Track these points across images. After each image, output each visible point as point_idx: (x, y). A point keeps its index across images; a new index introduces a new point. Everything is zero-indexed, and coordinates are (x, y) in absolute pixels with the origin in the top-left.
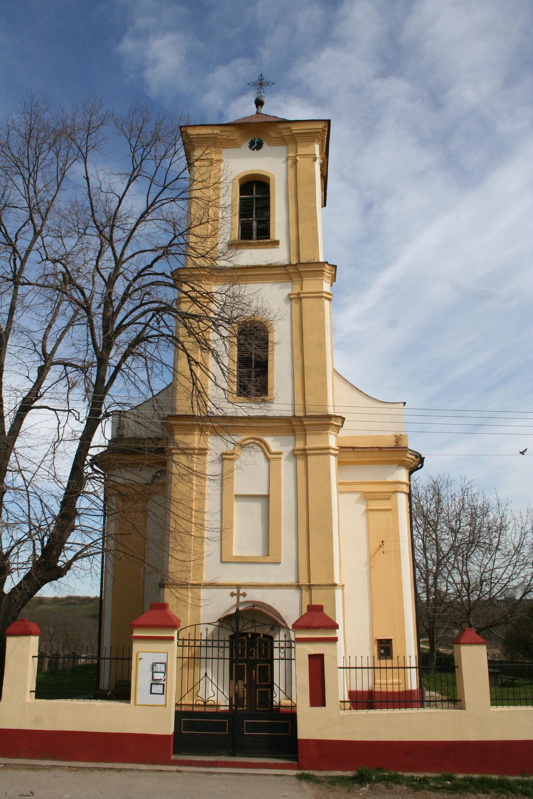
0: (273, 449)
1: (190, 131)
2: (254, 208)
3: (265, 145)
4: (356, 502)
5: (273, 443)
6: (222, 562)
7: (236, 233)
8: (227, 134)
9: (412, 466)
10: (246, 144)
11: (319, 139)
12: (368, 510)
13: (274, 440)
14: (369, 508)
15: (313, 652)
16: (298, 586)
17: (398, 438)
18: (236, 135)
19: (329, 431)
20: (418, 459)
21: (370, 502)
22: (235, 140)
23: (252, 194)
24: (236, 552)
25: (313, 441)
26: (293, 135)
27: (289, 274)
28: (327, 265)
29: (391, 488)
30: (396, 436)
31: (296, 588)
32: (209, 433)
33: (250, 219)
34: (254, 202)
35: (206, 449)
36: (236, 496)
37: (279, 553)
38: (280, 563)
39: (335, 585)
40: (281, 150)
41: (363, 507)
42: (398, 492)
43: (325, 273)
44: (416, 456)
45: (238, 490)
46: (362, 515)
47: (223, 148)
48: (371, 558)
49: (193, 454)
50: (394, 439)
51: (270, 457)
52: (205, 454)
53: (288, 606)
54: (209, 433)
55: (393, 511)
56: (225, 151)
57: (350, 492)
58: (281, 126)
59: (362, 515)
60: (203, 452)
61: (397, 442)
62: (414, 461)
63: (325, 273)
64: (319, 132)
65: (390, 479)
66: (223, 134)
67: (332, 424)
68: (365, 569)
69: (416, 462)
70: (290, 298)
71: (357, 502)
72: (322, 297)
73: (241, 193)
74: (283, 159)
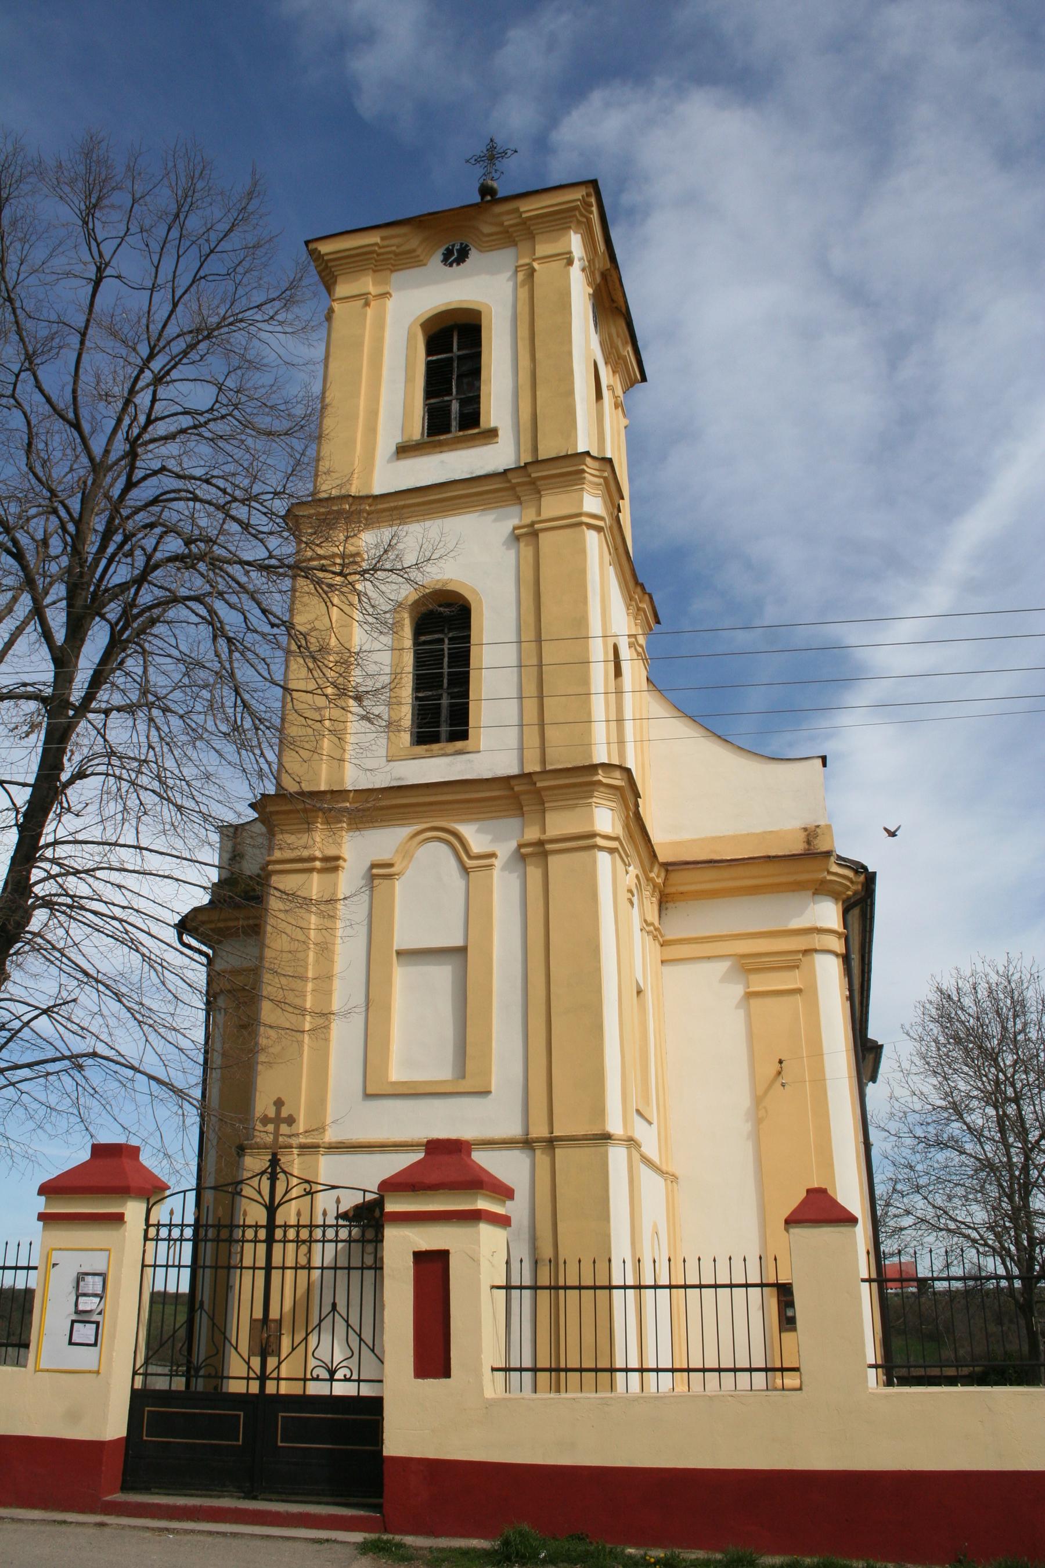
0: (476, 848)
2: (455, 377)
3: (474, 254)
4: (724, 979)
5: (476, 836)
6: (368, 1096)
7: (417, 429)
9: (850, 893)
10: (438, 256)
11: (579, 222)
12: (750, 995)
13: (478, 831)
14: (751, 989)
15: (424, 1246)
16: (527, 1143)
17: (811, 834)
18: (413, 241)
19: (594, 800)
20: (862, 878)
21: (753, 977)
22: (414, 251)
23: (451, 351)
24: (396, 1074)
25: (560, 823)
26: (524, 222)
27: (513, 488)
28: (588, 460)
30: (805, 829)
31: (522, 1148)
32: (345, 825)
33: (446, 398)
34: (455, 365)
35: (337, 858)
36: (399, 953)
37: (486, 1073)
38: (489, 1092)
39: (607, 1137)
40: (506, 258)
41: (738, 990)
42: (816, 951)
43: (586, 475)
44: (856, 872)
45: (402, 940)
46: (738, 1007)
47: (392, 271)
48: (758, 1101)
49: (311, 870)
50: (802, 836)
51: (470, 865)
52: (336, 869)
54: (345, 825)
55: (806, 993)
56: (395, 277)
57: (709, 958)
59: (738, 1007)
60: (332, 864)
61: (809, 842)
63: (586, 475)
64: (576, 208)
65: (795, 924)
66: (386, 243)
67: (600, 783)
68: (747, 1127)
69: (858, 883)
70: (516, 537)
71: (724, 979)
72: (581, 524)
73: (429, 352)
74: (509, 274)
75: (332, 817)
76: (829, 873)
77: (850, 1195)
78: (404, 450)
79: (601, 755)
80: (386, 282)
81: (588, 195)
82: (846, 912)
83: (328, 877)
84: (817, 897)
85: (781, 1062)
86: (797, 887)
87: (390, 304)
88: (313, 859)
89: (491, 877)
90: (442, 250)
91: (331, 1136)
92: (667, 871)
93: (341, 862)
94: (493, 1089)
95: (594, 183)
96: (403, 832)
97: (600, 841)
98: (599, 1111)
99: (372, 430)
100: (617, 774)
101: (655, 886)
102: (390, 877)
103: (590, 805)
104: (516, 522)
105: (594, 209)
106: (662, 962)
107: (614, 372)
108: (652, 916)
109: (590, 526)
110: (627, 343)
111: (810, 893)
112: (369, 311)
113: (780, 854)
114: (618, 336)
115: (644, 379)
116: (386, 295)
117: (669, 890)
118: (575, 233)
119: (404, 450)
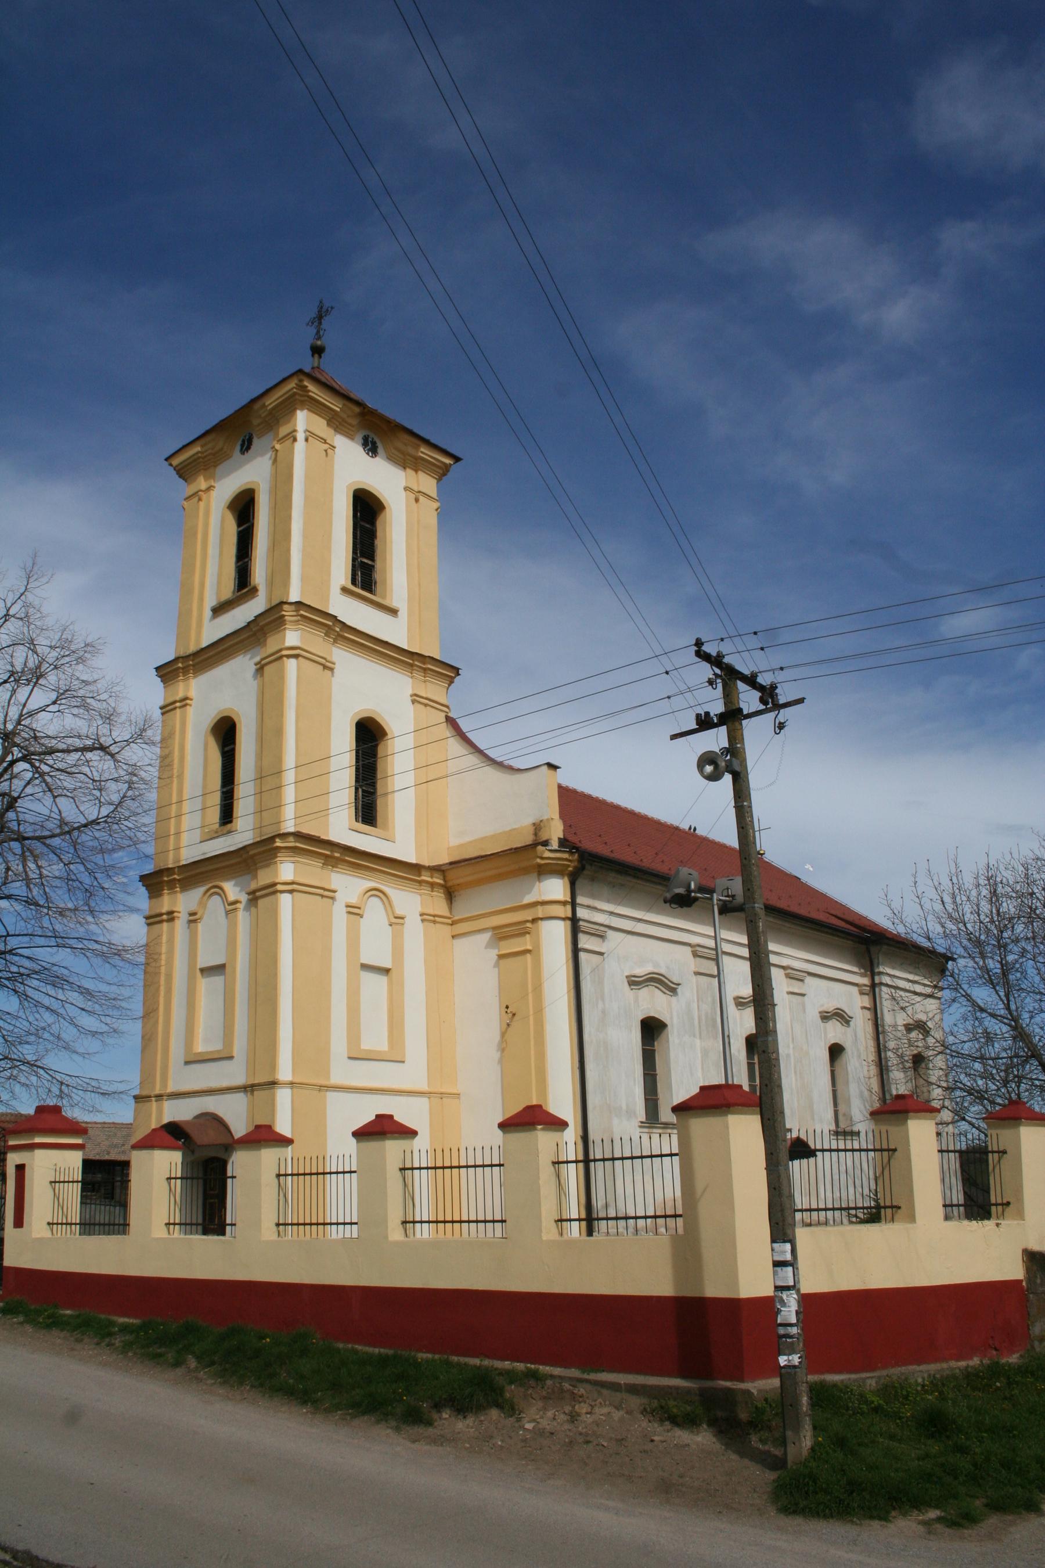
1: (176, 462)
3: (255, 441)
4: (488, 946)
5: (232, 890)
6: (187, 1063)
7: (228, 589)
8: (210, 446)
9: (570, 869)
10: (238, 447)
12: (501, 957)
15: (19, 1162)
17: (537, 827)
21: (503, 943)
26: (271, 412)
28: (286, 607)
29: (528, 915)
30: (534, 824)
36: (202, 970)
39: (273, 1084)
41: (493, 953)
42: (542, 919)
44: (571, 853)
45: (203, 961)
48: (503, 1034)
49: (161, 922)
50: (532, 830)
53: (237, 1116)
56: (220, 469)
58: (257, 406)
60: (171, 917)
61: (536, 834)
62: (570, 861)
64: (295, 394)
65: (528, 899)
68: (497, 1055)
71: (488, 946)
72: (281, 657)
75: (172, 885)
76: (542, 858)
77: (562, 1102)
78: (219, 610)
79: (289, 827)
80: (212, 477)
81: (301, 381)
82: (573, 885)
83: (170, 924)
84: (542, 877)
85: (507, 1007)
86: (525, 871)
87: (214, 494)
88: (161, 915)
89: (236, 916)
90: (240, 442)
91: (171, 1088)
92: (443, 871)
93: (175, 914)
94: (235, 1054)
96: (202, 890)
97: (279, 887)
98: (273, 1066)
100: (291, 839)
101: (432, 885)
102: (195, 921)
103: (276, 863)
104: (257, 659)
105: (311, 387)
106: (453, 937)
107: (416, 471)
108: (438, 904)
109: (289, 656)
110: (419, 446)
111: (535, 874)
112: (202, 504)
113: (519, 845)
114: (405, 444)
115: (457, 459)
116: (210, 488)
117: (450, 884)
118: (302, 409)
119: (219, 610)
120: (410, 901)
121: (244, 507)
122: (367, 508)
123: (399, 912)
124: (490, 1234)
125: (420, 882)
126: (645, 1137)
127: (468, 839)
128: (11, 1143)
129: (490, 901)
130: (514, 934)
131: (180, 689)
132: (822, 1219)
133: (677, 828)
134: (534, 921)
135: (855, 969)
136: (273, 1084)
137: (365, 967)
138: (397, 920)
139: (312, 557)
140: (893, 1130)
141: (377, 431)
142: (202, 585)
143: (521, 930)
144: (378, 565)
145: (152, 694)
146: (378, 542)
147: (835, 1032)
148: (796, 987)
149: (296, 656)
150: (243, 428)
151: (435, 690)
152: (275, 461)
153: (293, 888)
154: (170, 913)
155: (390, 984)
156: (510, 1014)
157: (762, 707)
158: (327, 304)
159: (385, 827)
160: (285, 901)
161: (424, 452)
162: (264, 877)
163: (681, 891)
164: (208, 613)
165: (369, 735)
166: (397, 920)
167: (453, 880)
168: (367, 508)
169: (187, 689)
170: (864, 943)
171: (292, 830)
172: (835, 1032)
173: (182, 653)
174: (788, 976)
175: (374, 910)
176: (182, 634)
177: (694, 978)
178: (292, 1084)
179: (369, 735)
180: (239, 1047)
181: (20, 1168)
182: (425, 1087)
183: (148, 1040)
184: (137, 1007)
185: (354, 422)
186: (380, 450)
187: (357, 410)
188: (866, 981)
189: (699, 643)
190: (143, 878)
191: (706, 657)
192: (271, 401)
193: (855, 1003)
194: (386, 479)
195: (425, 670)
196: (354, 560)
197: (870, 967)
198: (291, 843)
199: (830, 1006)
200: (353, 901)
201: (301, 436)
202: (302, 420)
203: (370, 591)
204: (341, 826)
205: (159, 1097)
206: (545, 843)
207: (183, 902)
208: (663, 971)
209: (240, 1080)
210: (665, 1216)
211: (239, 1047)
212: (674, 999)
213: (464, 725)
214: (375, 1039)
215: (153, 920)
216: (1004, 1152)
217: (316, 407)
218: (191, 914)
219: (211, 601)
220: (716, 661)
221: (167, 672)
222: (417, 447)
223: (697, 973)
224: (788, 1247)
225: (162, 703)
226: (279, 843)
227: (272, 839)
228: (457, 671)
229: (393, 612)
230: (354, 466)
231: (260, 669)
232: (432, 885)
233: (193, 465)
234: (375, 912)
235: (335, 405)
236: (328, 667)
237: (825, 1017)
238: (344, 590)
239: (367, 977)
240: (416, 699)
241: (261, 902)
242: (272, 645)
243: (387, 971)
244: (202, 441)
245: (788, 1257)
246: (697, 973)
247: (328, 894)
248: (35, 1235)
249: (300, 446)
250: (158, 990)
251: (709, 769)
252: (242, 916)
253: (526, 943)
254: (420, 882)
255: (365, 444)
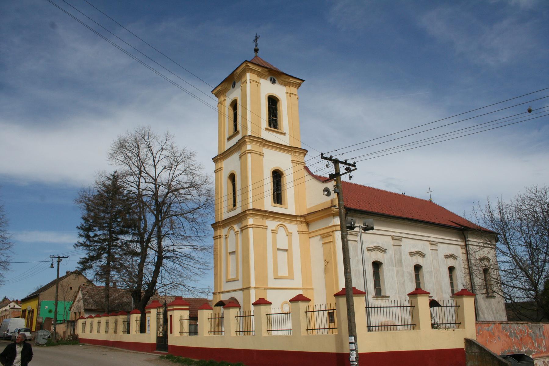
3: (236, 84)
4: (320, 240)
5: (236, 227)
12: (324, 244)
18: (226, 85)
21: (324, 239)
24: (230, 277)
36: (230, 253)
39: (249, 288)
45: (230, 250)
50: (330, 202)
58: (235, 73)
60: (220, 237)
65: (331, 225)
68: (323, 276)
71: (320, 240)
78: (229, 139)
86: (329, 216)
87: (226, 101)
91: (223, 290)
95: (246, 61)
99: (224, 136)
101: (301, 221)
105: (251, 66)
108: (304, 227)
109: (248, 153)
115: (303, 81)
116: (225, 100)
119: (229, 139)
120: (293, 227)
121: (234, 105)
122: (273, 102)
123: (290, 231)
124: (324, 333)
125: (297, 221)
126: (375, 301)
127: (312, 206)
128: (169, 308)
129: (319, 226)
130: (326, 236)
131: (219, 165)
132: (447, 327)
133: (397, 194)
134: (333, 231)
135: (459, 240)
136: (249, 288)
137: (278, 249)
138: (289, 234)
139: (255, 118)
140: (413, 300)
141: (275, 75)
142: (224, 131)
143: (328, 235)
144: (278, 119)
145: (212, 166)
146: (278, 112)
147: (451, 262)
148: (434, 247)
149: (250, 153)
150: (232, 80)
151: (299, 158)
152: (242, 90)
153: (253, 226)
154: (220, 236)
155: (288, 253)
156: (327, 262)
157: (346, 171)
158: (258, 35)
159: (285, 205)
160: (251, 231)
161: (291, 80)
162: (244, 224)
163: (349, 225)
164: (226, 140)
165: (277, 175)
166: (289, 234)
167: (307, 219)
168: (273, 102)
169: (221, 165)
170: (462, 229)
171: (252, 208)
172: (451, 262)
173: (220, 153)
174: (431, 244)
175: (281, 231)
176: (219, 148)
177: (393, 247)
178: (255, 288)
179: (277, 175)
180: (240, 278)
181: (171, 316)
182: (301, 287)
183: (216, 275)
184: (212, 265)
185: (266, 74)
186: (277, 81)
187: (267, 70)
188: (463, 244)
189: (322, 154)
190: (212, 225)
191: (325, 158)
192: (239, 71)
193: (459, 252)
194: (279, 90)
195: (296, 152)
196: (269, 118)
197: (465, 239)
198: (251, 212)
199: (448, 253)
200: (274, 229)
201: (248, 81)
202: (249, 76)
203: (277, 128)
204: (269, 205)
205: (219, 293)
206: (335, 206)
207: (223, 232)
208: (380, 245)
209: (241, 287)
210: (381, 326)
211: (240, 278)
212: (385, 255)
213: (310, 168)
214: (283, 271)
215: (215, 238)
216: (459, 306)
217: (253, 71)
218: (226, 236)
219: (227, 136)
220: (330, 159)
221: (216, 160)
222: (289, 79)
223: (394, 245)
224: (353, 338)
225: (214, 169)
226: (247, 213)
227: (245, 211)
228: (307, 151)
229: (284, 134)
230: (268, 88)
231: (240, 157)
232: (301, 221)
233: (219, 93)
234: (282, 232)
235: (259, 69)
236: (261, 155)
237: (447, 257)
238: (266, 129)
239: (279, 252)
240: (293, 162)
241: (244, 231)
242: (243, 150)
243: (287, 250)
244: (223, 84)
245: (353, 341)
246: (394, 245)
247: (265, 227)
248: (175, 336)
249: (248, 85)
250: (217, 259)
251: (326, 193)
252: (239, 236)
253: (330, 239)
254: (297, 221)
255: (271, 80)
